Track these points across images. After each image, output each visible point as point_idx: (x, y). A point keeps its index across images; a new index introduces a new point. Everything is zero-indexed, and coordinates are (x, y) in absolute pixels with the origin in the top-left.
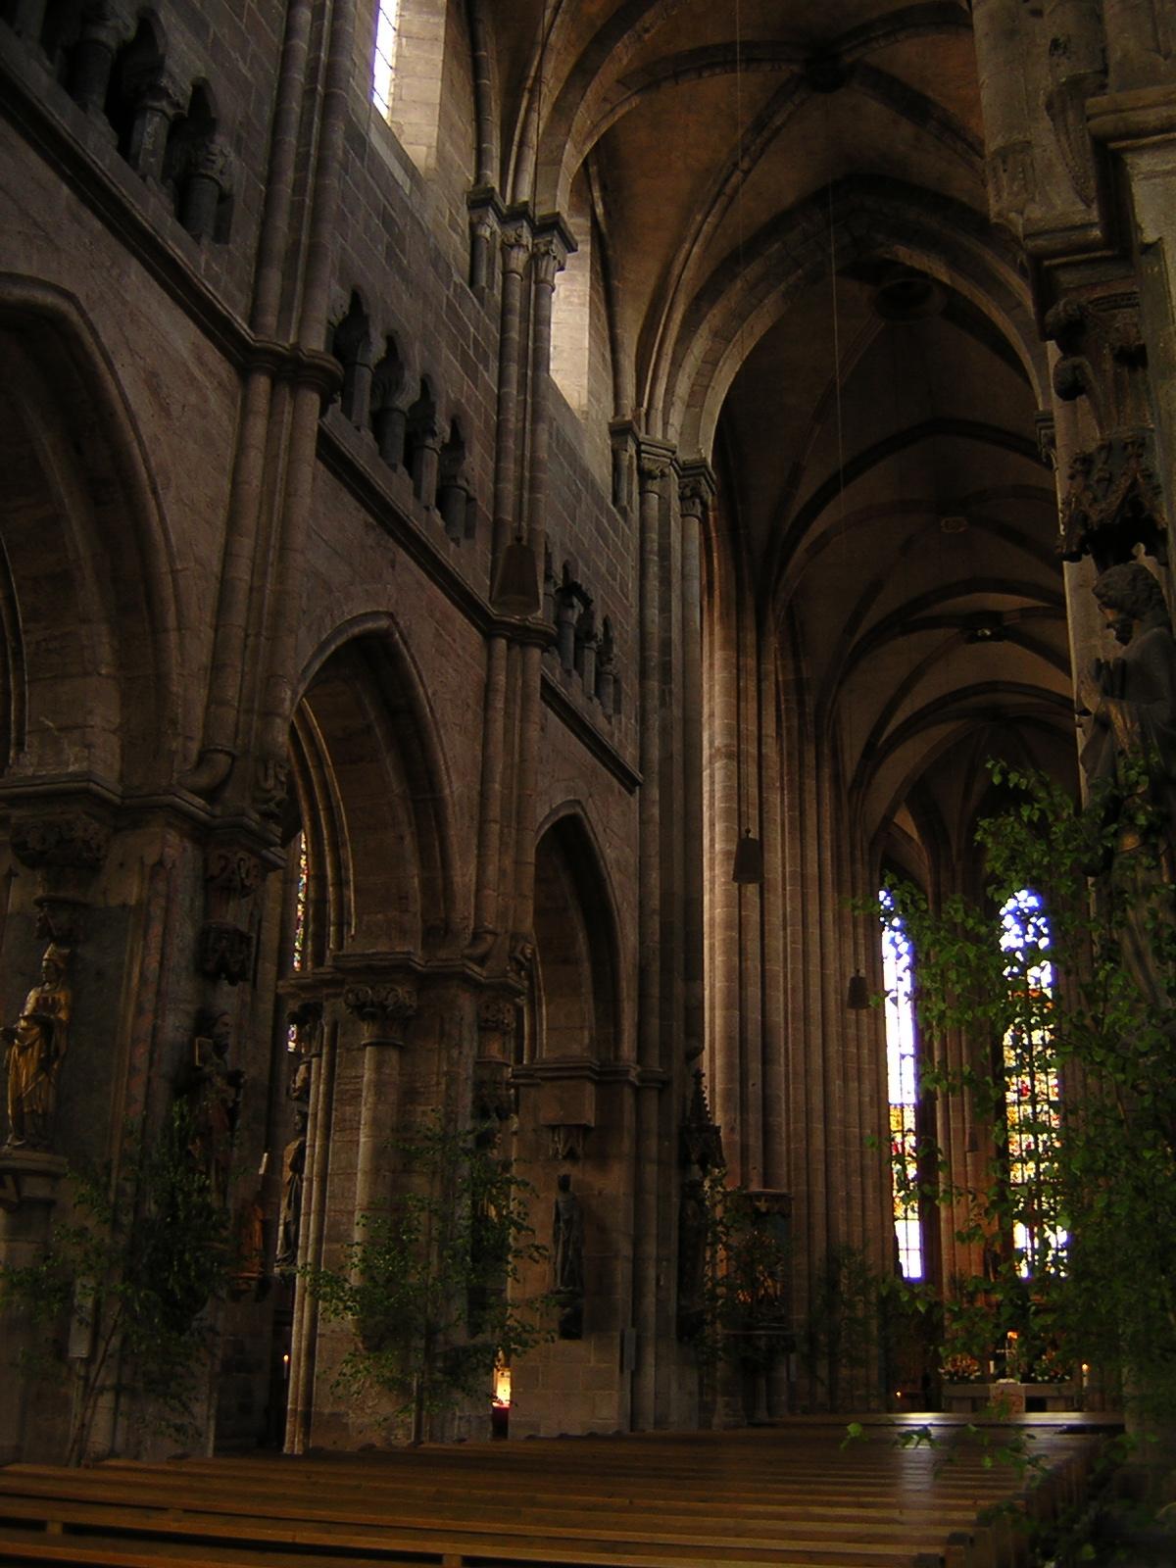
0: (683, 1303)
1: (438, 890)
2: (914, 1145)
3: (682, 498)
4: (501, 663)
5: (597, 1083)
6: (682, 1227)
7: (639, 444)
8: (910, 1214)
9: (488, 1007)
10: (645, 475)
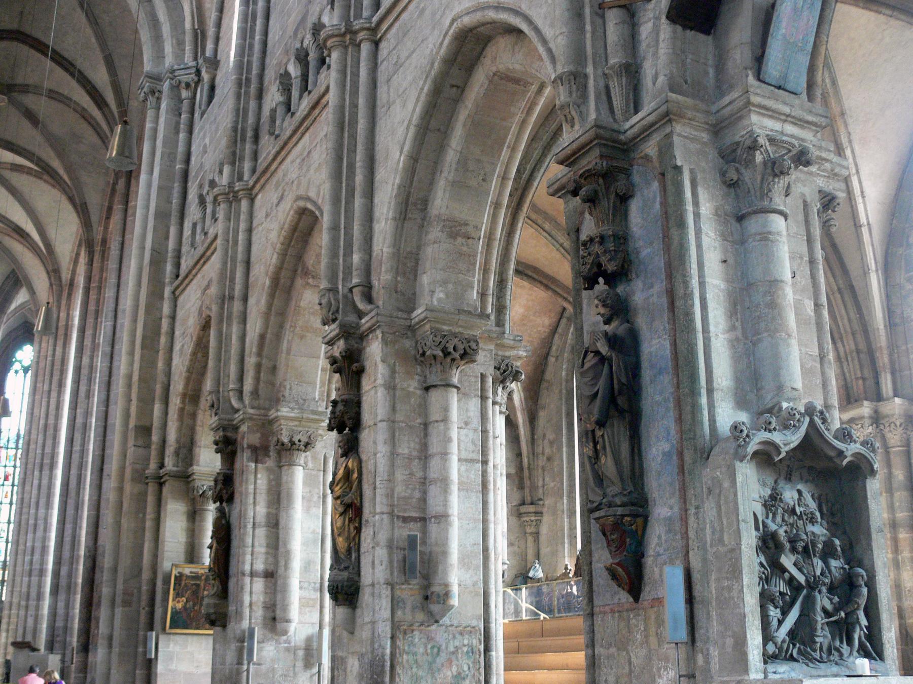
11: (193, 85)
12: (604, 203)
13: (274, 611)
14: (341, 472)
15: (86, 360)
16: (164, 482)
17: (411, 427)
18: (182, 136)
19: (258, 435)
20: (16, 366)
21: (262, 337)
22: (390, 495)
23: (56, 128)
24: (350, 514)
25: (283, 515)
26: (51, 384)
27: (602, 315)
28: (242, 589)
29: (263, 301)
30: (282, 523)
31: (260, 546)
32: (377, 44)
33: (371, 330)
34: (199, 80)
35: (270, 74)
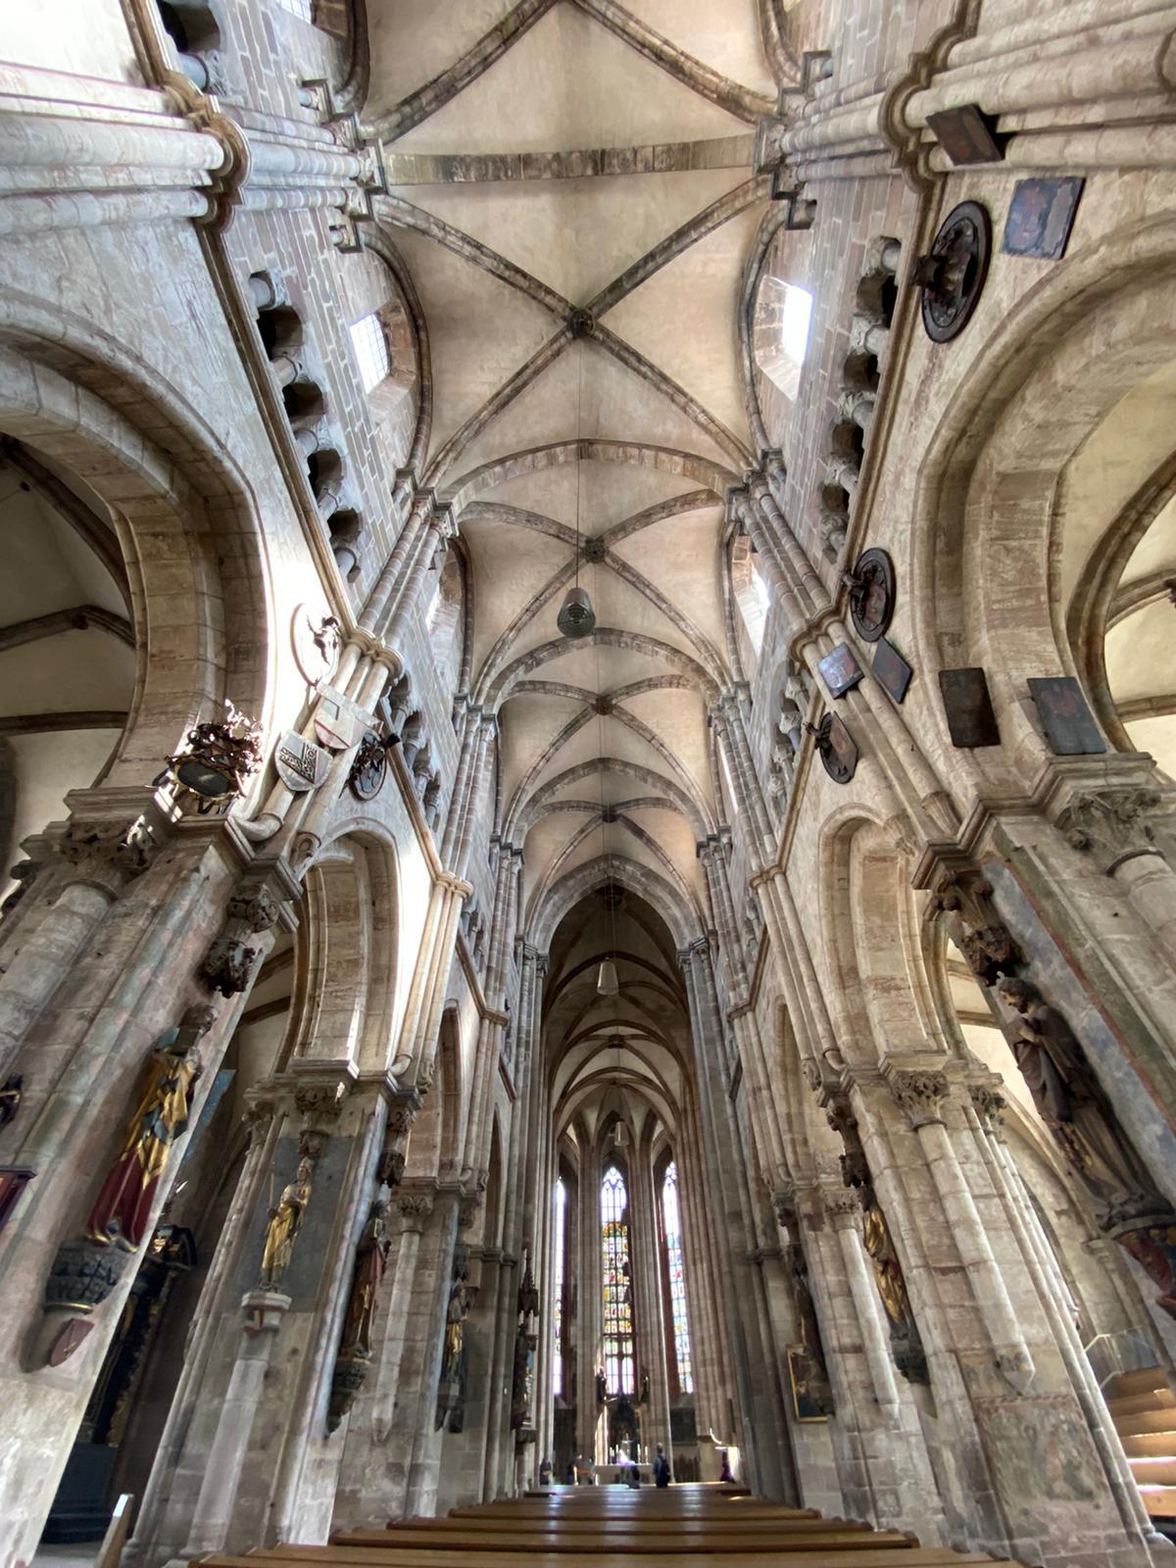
1: (449, 1145)
5: (484, 1262)
10: (525, 957)
12: (969, 904)
13: (874, 1391)
14: (868, 1226)
17: (914, 1170)
20: (668, 1181)
21: (789, 1116)
22: (918, 1245)
23: (650, 1005)
24: (890, 1272)
25: (852, 1280)
27: (1015, 1005)
29: (781, 1086)
30: (855, 1289)
32: (784, 874)
33: (850, 1085)
35: (740, 924)
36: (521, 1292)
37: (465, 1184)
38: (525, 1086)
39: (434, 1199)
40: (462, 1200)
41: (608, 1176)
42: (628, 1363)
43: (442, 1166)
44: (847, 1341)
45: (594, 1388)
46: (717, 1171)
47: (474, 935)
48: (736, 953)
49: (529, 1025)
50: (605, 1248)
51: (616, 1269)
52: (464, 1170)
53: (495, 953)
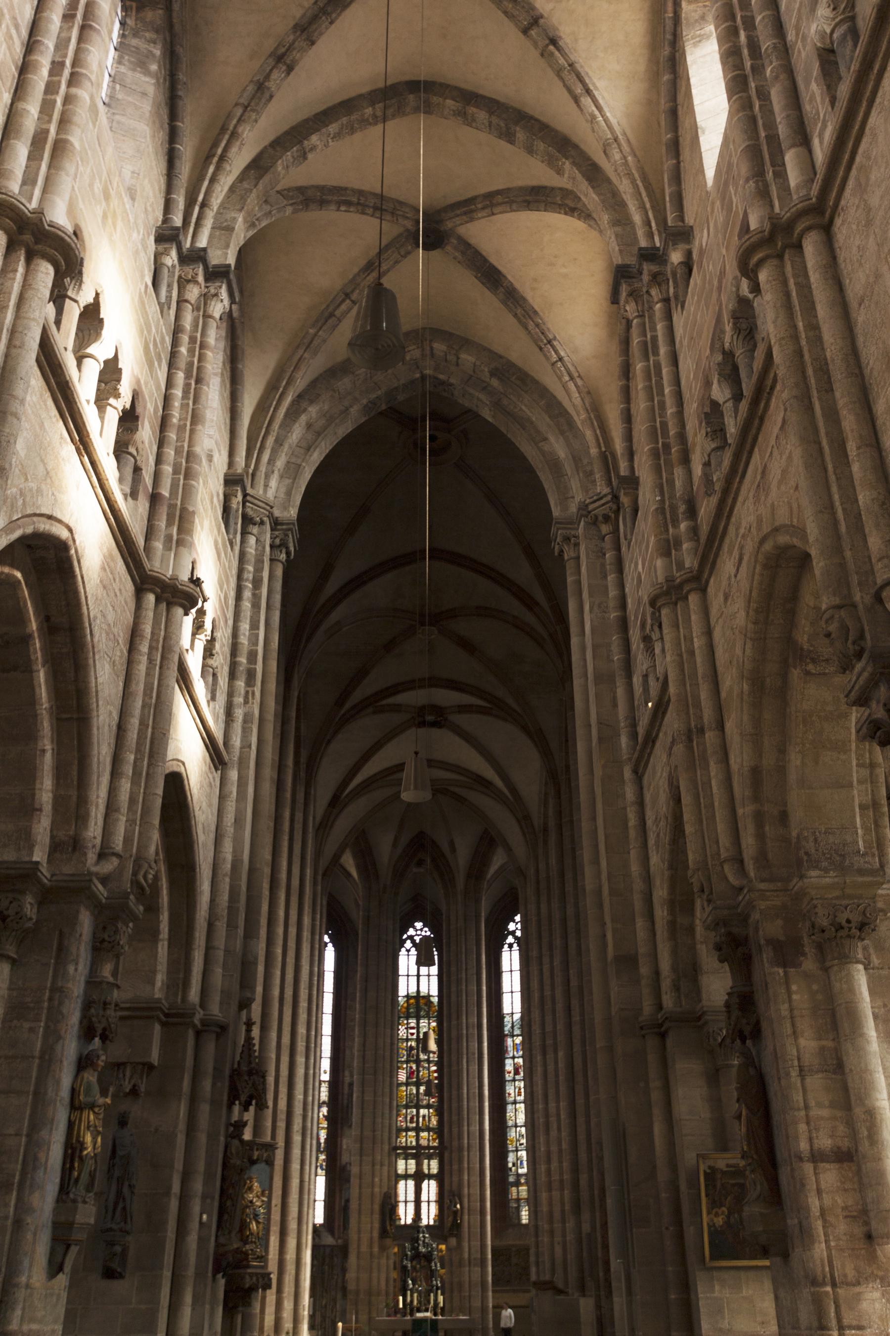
0: (222, 1240)
2: (326, 1114)
3: (272, 546)
4: (149, 614)
5: (163, 1024)
6: (225, 1165)
7: (245, 495)
8: (319, 1171)
9: (104, 928)
10: (247, 520)
11: (613, 516)
15: (570, 911)
16: (666, 1032)
18: (611, 578)
19: (780, 922)
20: (510, 939)
21: (756, 772)
26: (540, 948)
28: (803, 1185)
31: (819, 1105)
34: (619, 509)
35: (692, 423)
36: (235, 1074)
37: (104, 880)
38: (245, 745)
39: (41, 903)
40: (98, 909)
41: (411, 932)
42: (430, 1189)
43: (55, 847)
44: (825, 1142)
45: (377, 1217)
46: (599, 892)
47: (113, 417)
48: (678, 484)
49: (254, 640)
50: (402, 1032)
51: (418, 1062)
52: (102, 855)
53: (168, 469)
